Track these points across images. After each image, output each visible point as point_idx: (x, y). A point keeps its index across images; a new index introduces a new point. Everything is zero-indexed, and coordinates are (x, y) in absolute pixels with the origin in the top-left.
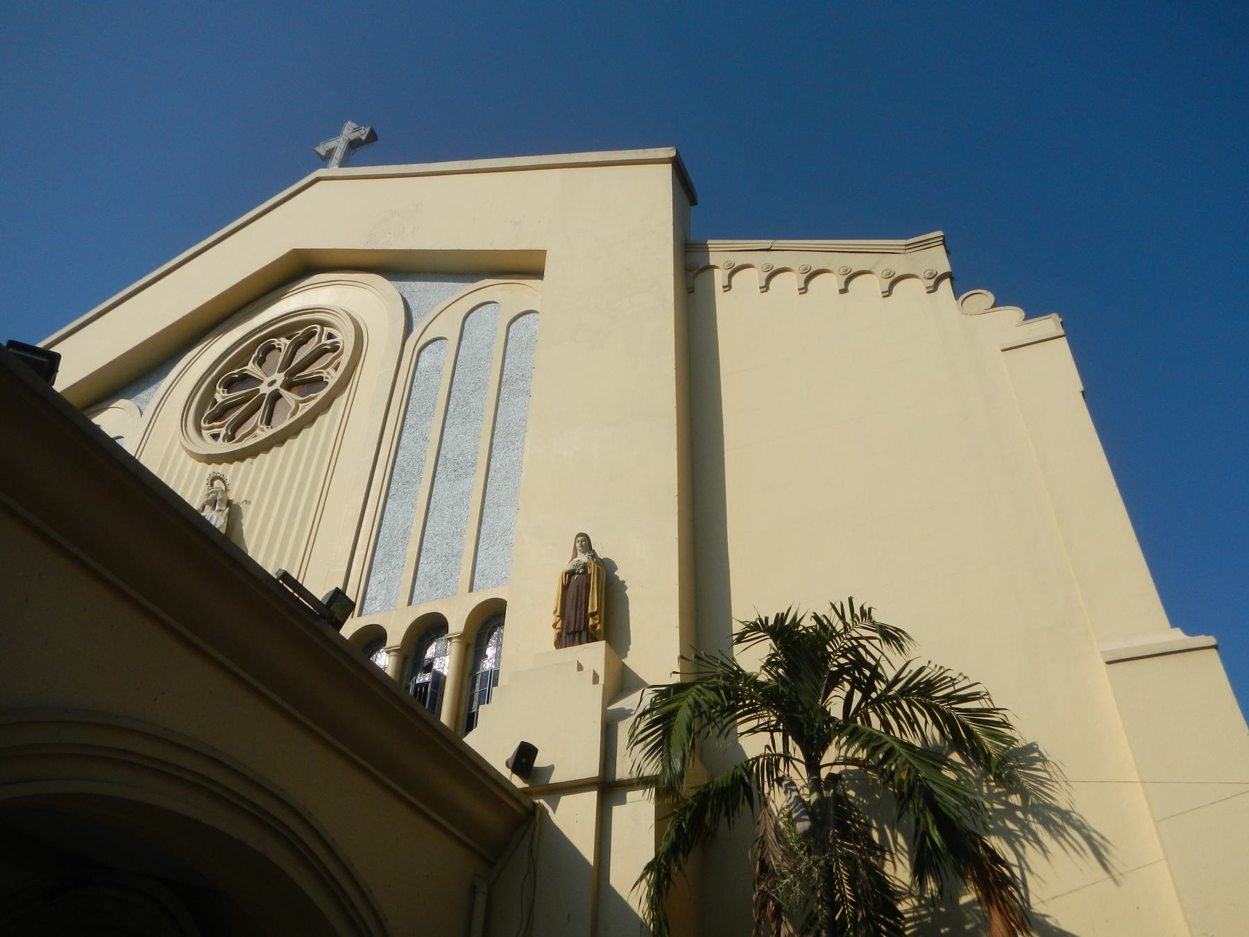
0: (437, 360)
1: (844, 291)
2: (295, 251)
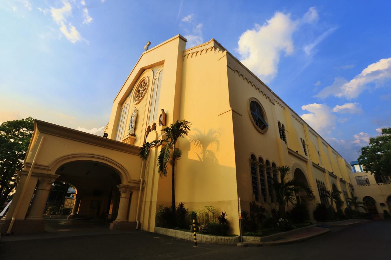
0: (156, 82)
1: (201, 54)
2: (141, 68)
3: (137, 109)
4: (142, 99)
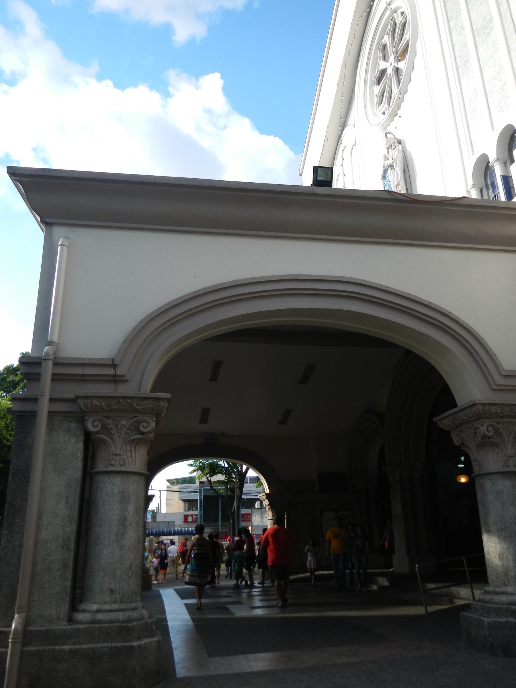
3: (399, 137)
4: (403, 93)
